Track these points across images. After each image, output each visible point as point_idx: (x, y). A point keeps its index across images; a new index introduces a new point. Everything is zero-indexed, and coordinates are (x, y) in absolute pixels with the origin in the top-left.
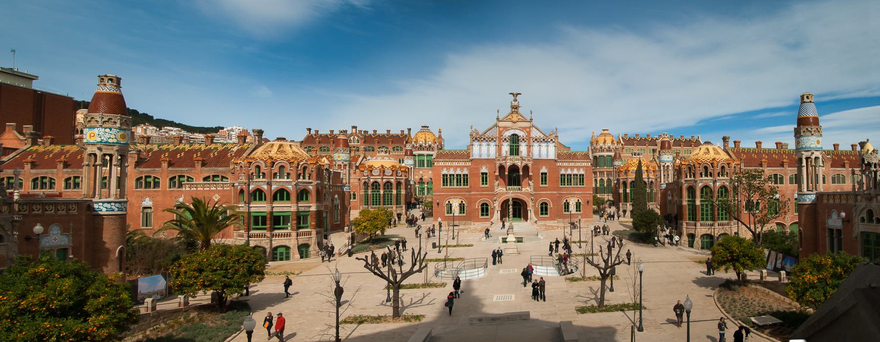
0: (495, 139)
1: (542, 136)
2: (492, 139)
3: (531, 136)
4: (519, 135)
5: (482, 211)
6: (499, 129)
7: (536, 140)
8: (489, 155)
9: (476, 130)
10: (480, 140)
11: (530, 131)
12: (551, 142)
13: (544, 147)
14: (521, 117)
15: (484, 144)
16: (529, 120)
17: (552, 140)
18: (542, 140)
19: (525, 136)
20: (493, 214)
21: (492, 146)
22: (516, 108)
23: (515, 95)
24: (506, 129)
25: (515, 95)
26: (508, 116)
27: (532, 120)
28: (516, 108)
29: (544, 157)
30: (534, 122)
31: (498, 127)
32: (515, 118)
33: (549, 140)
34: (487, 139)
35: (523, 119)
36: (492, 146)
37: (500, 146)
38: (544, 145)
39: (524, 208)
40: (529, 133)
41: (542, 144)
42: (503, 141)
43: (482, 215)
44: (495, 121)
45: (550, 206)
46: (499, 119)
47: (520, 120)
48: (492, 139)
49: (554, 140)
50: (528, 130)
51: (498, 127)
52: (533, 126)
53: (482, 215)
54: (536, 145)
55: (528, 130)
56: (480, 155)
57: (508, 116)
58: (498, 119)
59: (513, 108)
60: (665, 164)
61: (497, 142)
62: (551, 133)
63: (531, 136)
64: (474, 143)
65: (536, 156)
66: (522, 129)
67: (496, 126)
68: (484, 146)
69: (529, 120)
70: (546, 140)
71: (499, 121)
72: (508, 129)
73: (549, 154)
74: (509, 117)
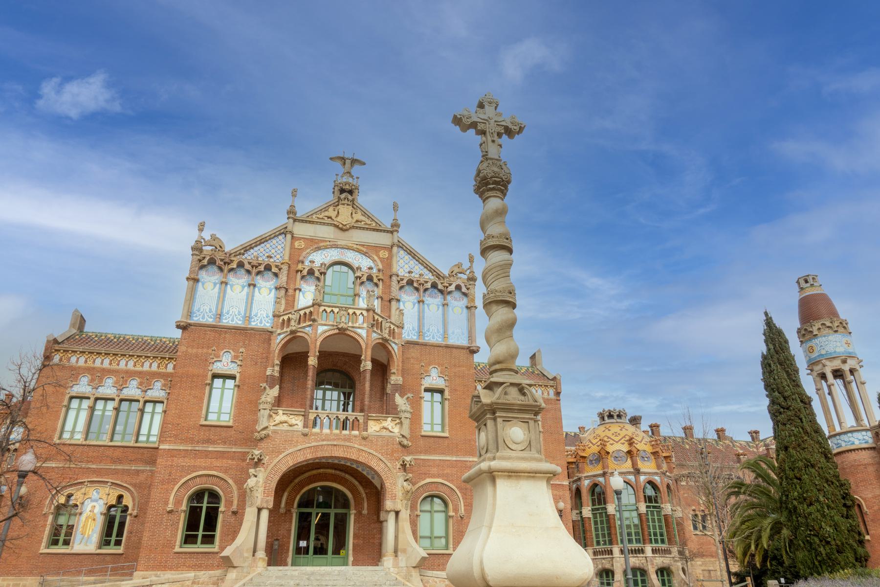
0: (274, 270)
1: (429, 276)
2: (268, 268)
3: (394, 270)
4: (355, 264)
5: (192, 524)
6: (292, 244)
7: (410, 282)
8: (248, 318)
9: (214, 238)
10: (226, 268)
11: (390, 258)
12: (457, 294)
13: (433, 307)
14: (363, 218)
15: (238, 282)
16: (389, 227)
17: (458, 288)
18: (429, 285)
19: (375, 271)
20: (233, 533)
21: (265, 291)
22: (351, 192)
23: (348, 162)
24: (317, 244)
25: (348, 162)
26: (326, 209)
27: (398, 226)
28: (351, 192)
29: (433, 336)
30: (403, 235)
31: (289, 236)
32: (345, 215)
33: (452, 288)
34: (247, 267)
35: (370, 223)
36: (265, 291)
37: (291, 292)
38: (433, 302)
39: (359, 514)
40: (388, 263)
41: (428, 299)
42: (303, 277)
43: (189, 539)
44: (281, 220)
45: (456, 510)
46: (295, 214)
47: (362, 225)
48: (268, 268)
49: (464, 290)
50: (384, 254)
51: (289, 236)
52: (401, 246)
53: (189, 539)
54: (408, 301)
55: (384, 254)
56: (219, 316)
57: (326, 209)
58: (291, 212)
59: (342, 191)
60: (844, 362)
61: (283, 277)
62: (456, 270)
63: (394, 270)
64: (203, 275)
65: (409, 333)
66: (366, 250)
67: (284, 232)
68: (238, 288)
69: (389, 227)
70: (440, 287)
71: (295, 220)
72: (322, 244)
73: (450, 332)
74: (327, 214)
